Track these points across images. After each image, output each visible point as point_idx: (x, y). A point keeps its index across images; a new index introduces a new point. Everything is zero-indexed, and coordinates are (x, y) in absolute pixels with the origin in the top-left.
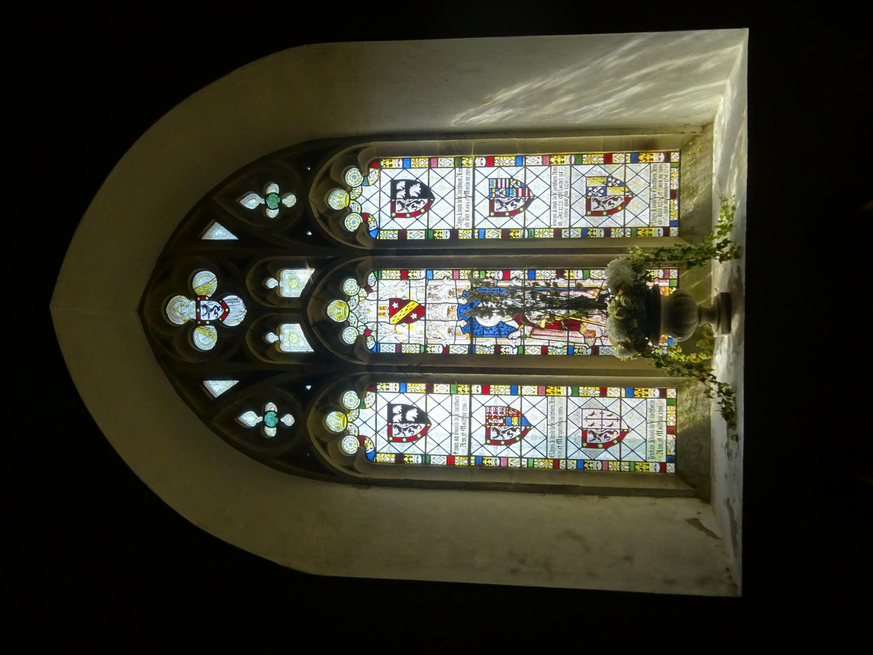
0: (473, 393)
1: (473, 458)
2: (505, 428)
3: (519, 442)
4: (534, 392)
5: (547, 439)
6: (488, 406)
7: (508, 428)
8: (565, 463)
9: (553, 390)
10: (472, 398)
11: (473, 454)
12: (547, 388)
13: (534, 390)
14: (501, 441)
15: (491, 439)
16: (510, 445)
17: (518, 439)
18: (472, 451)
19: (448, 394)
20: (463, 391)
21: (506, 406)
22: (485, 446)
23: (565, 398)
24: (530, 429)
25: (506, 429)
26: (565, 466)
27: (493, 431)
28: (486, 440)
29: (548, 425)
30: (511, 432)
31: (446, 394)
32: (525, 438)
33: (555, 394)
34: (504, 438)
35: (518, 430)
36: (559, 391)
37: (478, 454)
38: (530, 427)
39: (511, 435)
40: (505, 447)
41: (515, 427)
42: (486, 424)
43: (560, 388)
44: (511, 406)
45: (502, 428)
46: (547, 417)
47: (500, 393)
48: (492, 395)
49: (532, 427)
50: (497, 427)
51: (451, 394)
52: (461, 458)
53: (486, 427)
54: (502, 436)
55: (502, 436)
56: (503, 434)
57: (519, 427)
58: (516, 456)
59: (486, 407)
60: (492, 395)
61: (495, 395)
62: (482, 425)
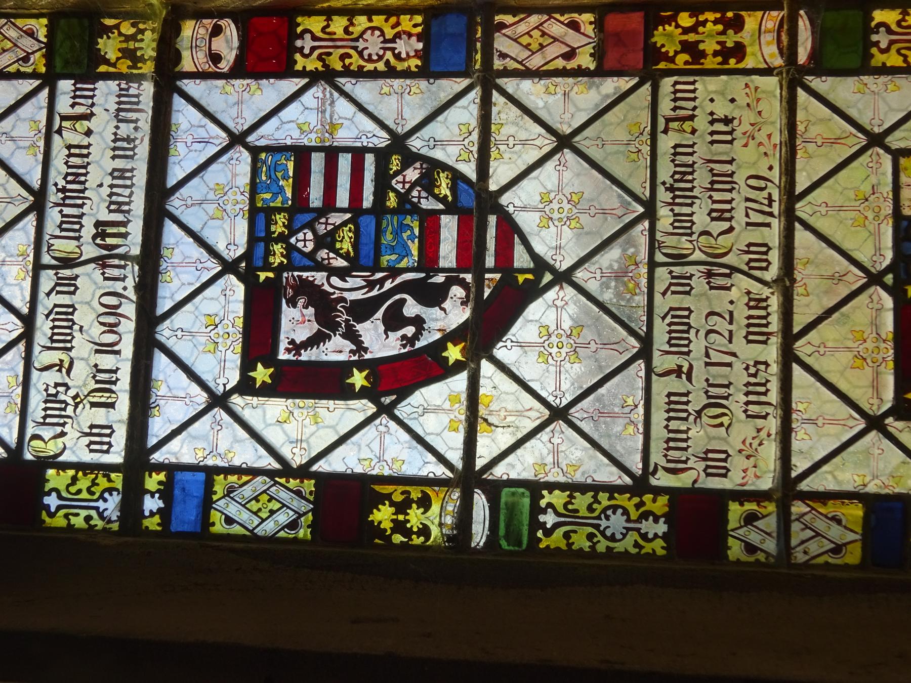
0: (187, 65)
1: (153, 481)
2: (371, 285)
3: (460, 382)
4: (570, 55)
5: (645, 353)
6: (268, 149)
7: (388, 285)
8: (770, 523)
9: (693, 29)
10: (178, 102)
11: (158, 457)
12: (653, 22)
13: (575, 40)
14: (345, 368)
15: (283, 356)
16: (404, 393)
17: (454, 353)
18: (158, 428)
19: (34, 75)
20: (130, 54)
21: (381, 139)
22: (237, 401)
23: (771, 83)
24: (533, 291)
25: (375, 292)
26: (771, 546)
27: (292, 303)
28: (247, 366)
29: (652, 265)
30: (412, 308)
31: (19, 75)
32: (500, 352)
33: (711, 63)
34: (360, 348)
35: (457, 291)
36: (731, 40)
37: (187, 458)
38: (539, 275)
39: (410, 331)
40: (367, 407)
41: (440, 279)
42: (247, 256)
43: (737, 25)
44: (416, 144)
45: (351, 282)
46: (650, 213)
47: (355, 61)
48: (303, 74)
49: (548, 277)
50: (319, 277)
51: (49, 80)
52: (84, 483)
53: (248, 278)
54: (352, 336)
55: (352, 336)
56: (361, 319)
57: (469, 277)
58: (441, 471)
59: (255, 151)
60: (303, 74)
61: (314, 78)
62: (229, 267)
